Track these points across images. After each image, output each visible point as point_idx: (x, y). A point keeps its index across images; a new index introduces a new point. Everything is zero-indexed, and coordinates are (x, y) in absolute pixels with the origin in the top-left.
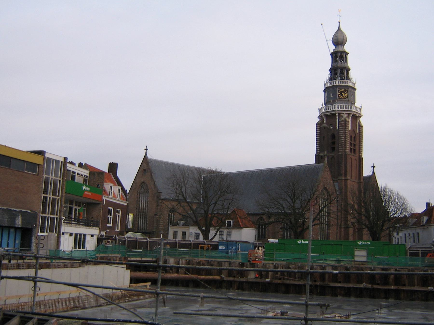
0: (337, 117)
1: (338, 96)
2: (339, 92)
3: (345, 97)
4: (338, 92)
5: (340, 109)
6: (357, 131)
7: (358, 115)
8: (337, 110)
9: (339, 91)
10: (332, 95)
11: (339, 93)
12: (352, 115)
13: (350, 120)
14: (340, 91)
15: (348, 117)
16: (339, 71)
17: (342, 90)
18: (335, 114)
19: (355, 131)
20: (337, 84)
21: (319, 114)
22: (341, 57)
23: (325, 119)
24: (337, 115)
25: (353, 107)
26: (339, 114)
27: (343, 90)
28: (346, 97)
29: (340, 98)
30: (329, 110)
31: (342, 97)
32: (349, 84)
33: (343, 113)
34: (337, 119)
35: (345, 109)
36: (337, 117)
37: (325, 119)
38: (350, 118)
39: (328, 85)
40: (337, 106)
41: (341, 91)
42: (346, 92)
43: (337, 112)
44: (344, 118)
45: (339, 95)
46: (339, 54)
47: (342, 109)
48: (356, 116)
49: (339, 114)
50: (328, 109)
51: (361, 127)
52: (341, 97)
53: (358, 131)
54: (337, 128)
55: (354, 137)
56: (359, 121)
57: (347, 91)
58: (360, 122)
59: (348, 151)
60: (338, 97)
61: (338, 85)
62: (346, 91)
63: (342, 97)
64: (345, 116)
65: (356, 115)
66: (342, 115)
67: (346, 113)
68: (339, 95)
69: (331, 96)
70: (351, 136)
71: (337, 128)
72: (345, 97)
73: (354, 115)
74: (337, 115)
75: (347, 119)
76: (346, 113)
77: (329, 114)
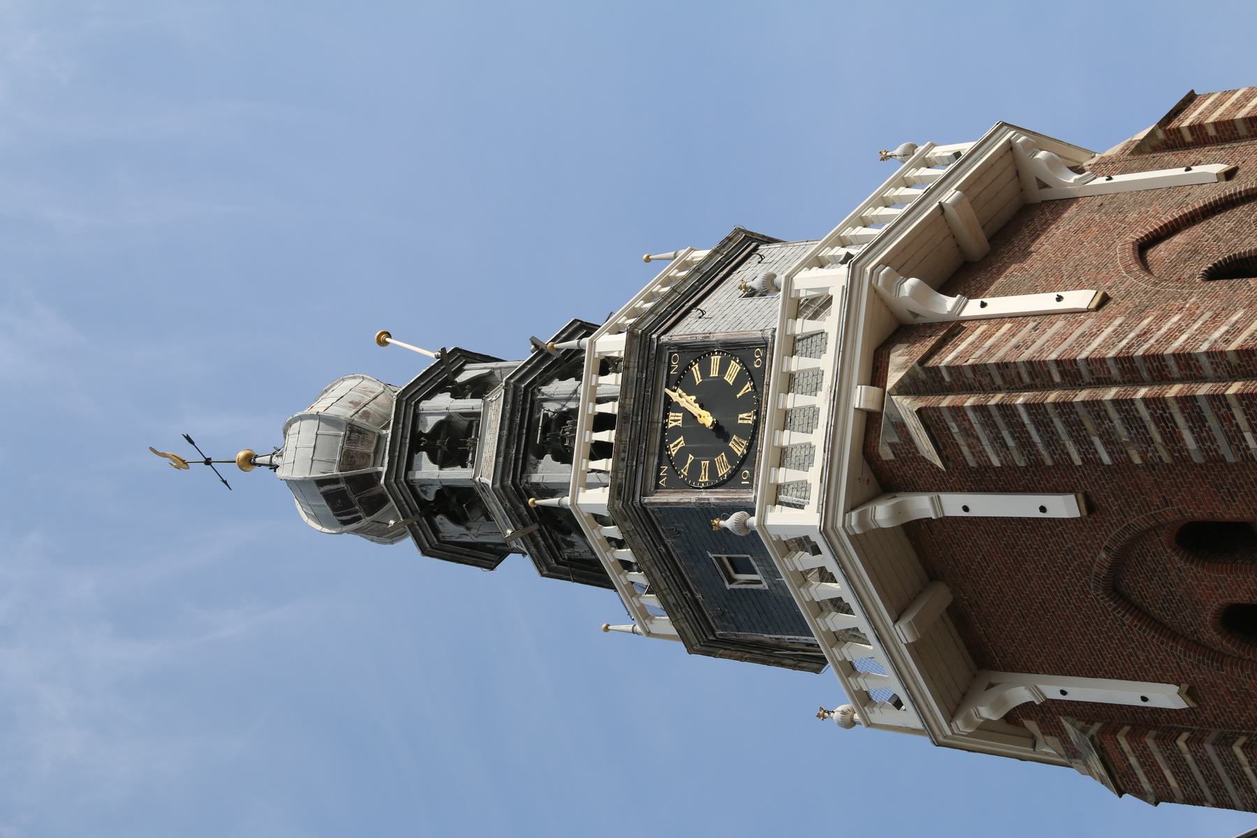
0: (922, 505)
1: (722, 484)
3: (748, 387)
7: (950, 196)
17: (677, 432)
18: (867, 541)
23: (1020, 692)
24: (881, 513)
33: (870, 420)
36: (922, 505)
40: (780, 519)
45: (713, 470)
46: (427, 470)
54: (1063, 507)
60: (731, 480)
63: (742, 431)
68: (713, 470)
71: (1063, 507)
76: (876, 376)
77: (903, 633)
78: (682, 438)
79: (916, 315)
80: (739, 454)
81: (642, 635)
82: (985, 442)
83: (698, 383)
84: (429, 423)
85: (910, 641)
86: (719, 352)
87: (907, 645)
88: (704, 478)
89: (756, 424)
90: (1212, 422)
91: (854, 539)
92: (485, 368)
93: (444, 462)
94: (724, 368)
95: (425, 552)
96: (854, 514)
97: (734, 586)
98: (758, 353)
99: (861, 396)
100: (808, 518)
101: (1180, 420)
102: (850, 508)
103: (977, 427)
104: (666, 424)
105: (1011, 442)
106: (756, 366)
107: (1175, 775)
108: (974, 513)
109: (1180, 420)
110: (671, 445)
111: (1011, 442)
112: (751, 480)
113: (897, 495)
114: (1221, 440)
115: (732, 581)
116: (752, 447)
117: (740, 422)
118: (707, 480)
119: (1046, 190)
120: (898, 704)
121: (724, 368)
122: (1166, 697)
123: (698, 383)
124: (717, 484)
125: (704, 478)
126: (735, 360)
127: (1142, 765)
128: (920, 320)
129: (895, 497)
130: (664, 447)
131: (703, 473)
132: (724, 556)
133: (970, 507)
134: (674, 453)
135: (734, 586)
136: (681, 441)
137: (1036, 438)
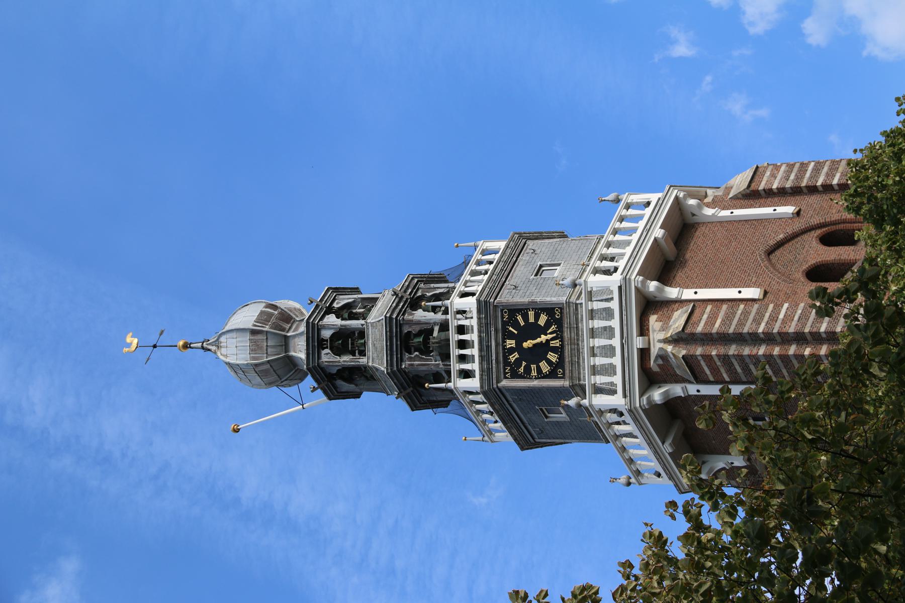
2: (522, 370)
3: (553, 328)
4: (521, 377)
7: (658, 233)
8: (625, 396)
9: (515, 375)
11: (528, 370)
12: (653, 285)
13: (688, 294)
14: (518, 362)
17: (511, 351)
18: (652, 411)
20: (474, 383)
24: (657, 395)
26: (650, 379)
27: (510, 343)
28: (548, 324)
29: (561, 363)
31: (554, 350)
33: (644, 353)
34: (692, 389)
35: (616, 342)
36: (677, 390)
38: (672, 292)
41: (516, 355)
47: (617, 361)
49: (650, 379)
52: (553, 357)
60: (552, 375)
61: (486, 373)
65: (655, 239)
67: (643, 330)
68: (539, 370)
74: (657, 395)
75: (678, 320)
78: (516, 353)
79: (655, 297)
80: (554, 361)
81: (488, 442)
83: (522, 325)
84: (327, 334)
85: (670, 451)
86: (533, 309)
87: (670, 454)
88: (534, 373)
89: (562, 346)
91: (644, 411)
92: (350, 298)
94: (537, 317)
96: (645, 398)
97: (548, 420)
98: (557, 310)
99: (638, 342)
100: (617, 400)
102: (641, 395)
104: (506, 346)
106: (557, 317)
108: (702, 393)
110: (510, 357)
112: (564, 374)
113: (661, 385)
115: (547, 417)
116: (561, 358)
117: (551, 345)
118: (536, 374)
119: (694, 217)
120: (659, 475)
121: (537, 317)
123: (522, 325)
124: (541, 375)
125: (534, 373)
126: (543, 314)
128: (657, 299)
129: (660, 387)
130: (506, 358)
131: (533, 371)
132: (543, 408)
133: (700, 390)
134: (512, 361)
135: (548, 420)
136: (516, 355)
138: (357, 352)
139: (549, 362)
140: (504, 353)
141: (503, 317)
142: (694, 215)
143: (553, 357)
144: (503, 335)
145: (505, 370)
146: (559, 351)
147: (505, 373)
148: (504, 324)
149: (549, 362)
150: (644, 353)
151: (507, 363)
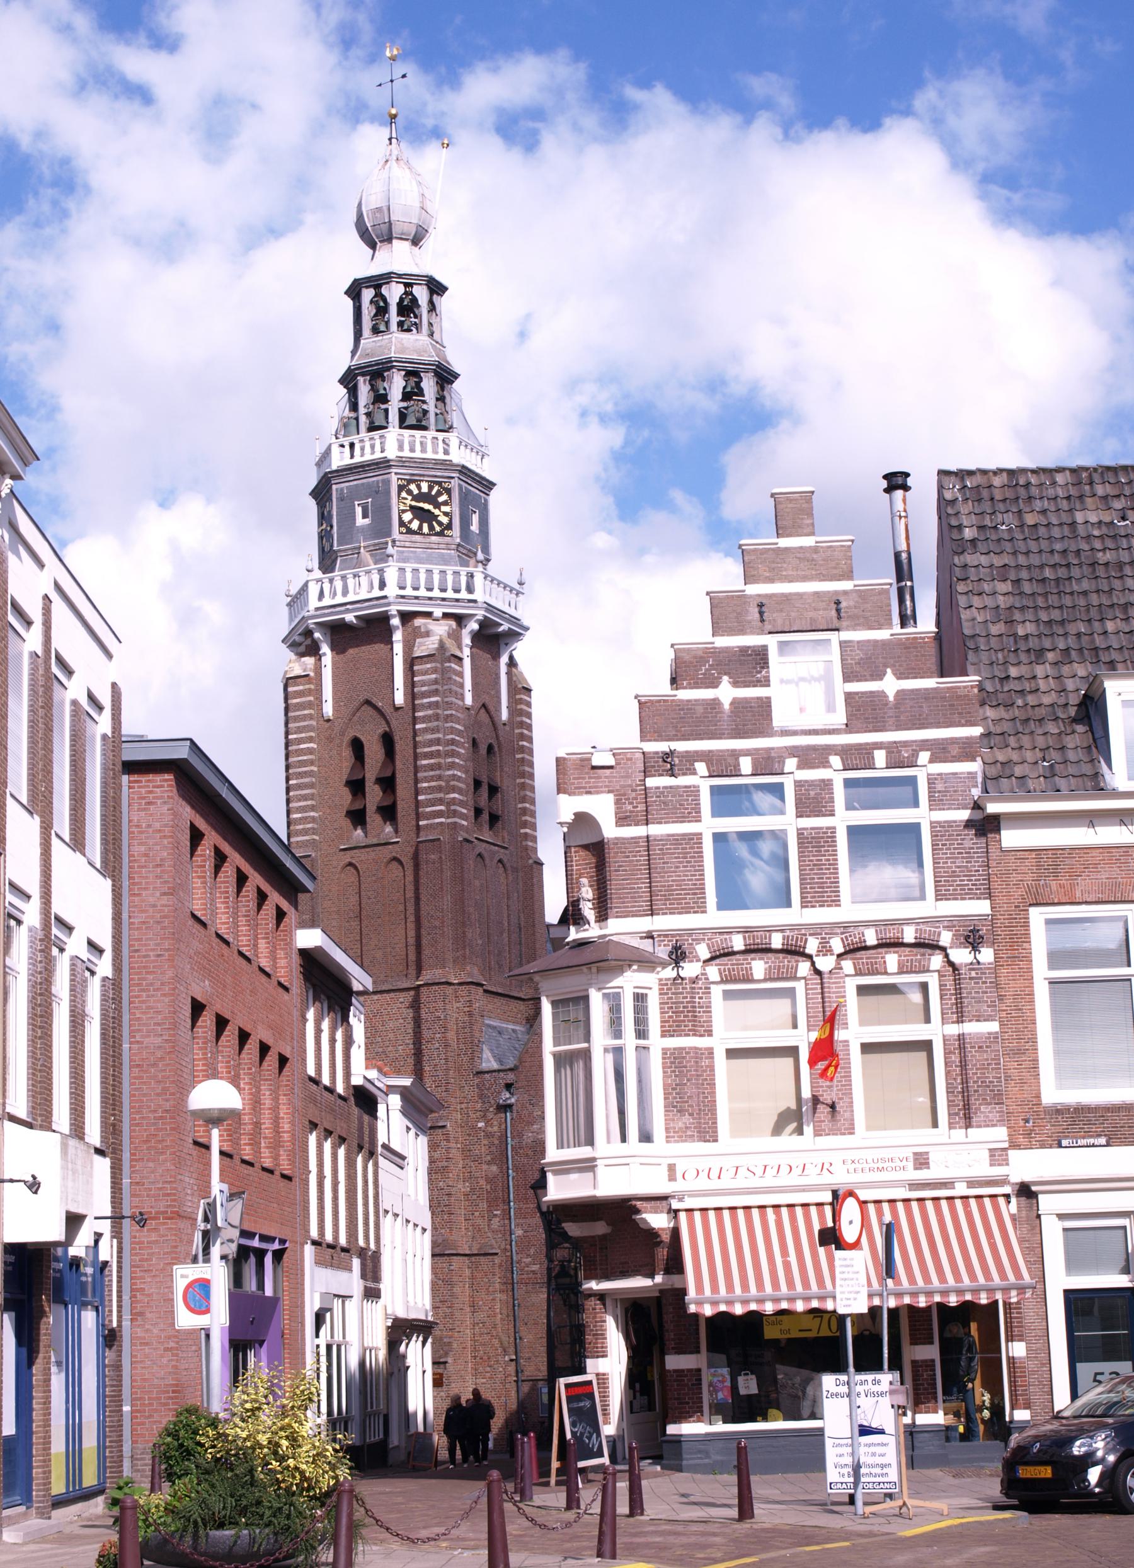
1: (400, 518)
3: (438, 529)
5: (409, 592)
6: (499, 710)
7: (505, 627)
10: (365, 516)
12: (475, 626)
13: (467, 652)
15: (456, 636)
16: (396, 385)
17: (419, 487)
18: (385, 618)
19: (492, 709)
21: (291, 620)
22: (408, 307)
24: (395, 621)
25: (478, 579)
27: (425, 488)
29: (410, 532)
30: (351, 597)
31: (420, 527)
32: (458, 456)
33: (428, 615)
34: (398, 648)
36: (398, 636)
37: (325, 649)
38: (467, 640)
39: (339, 459)
42: (441, 499)
43: (393, 610)
44: (438, 638)
48: (501, 629)
49: (407, 617)
50: (345, 592)
51: (521, 691)
52: (415, 525)
53: (505, 715)
54: (399, 698)
55: (490, 748)
56: (511, 658)
57: (449, 492)
58: (512, 663)
59: (465, 823)
60: (402, 523)
61: (402, 462)
62: (439, 494)
63: (420, 527)
64: (440, 629)
66: (418, 622)
69: (360, 521)
70: (474, 743)
71: (399, 698)
72: (438, 529)
73: (485, 624)
74: (395, 621)
76: (446, 616)
77: (350, 618)
82: (424, 678)
90: (432, 773)
93: (400, 304)
95: (356, 280)
99: (438, 612)
100: (392, 591)
101: (432, 761)
102: (398, 611)
103: (428, 677)
105: (424, 689)
107: (298, 703)
109: (432, 761)
111: (424, 689)
112: (402, 533)
114: (426, 774)
122: (328, 709)
127: (301, 691)
137: (425, 701)
138: (403, 319)
139: (410, 522)
140: (417, 481)
141: (445, 482)
142: (507, 644)
143: (415, 525)
144: (431, 482)
145: (405, 479)
146: (419, 532)
147: (401, 479)
148: (439, 484)
149: (410, 522)
150: (428, 615)
151: (410, 482)
